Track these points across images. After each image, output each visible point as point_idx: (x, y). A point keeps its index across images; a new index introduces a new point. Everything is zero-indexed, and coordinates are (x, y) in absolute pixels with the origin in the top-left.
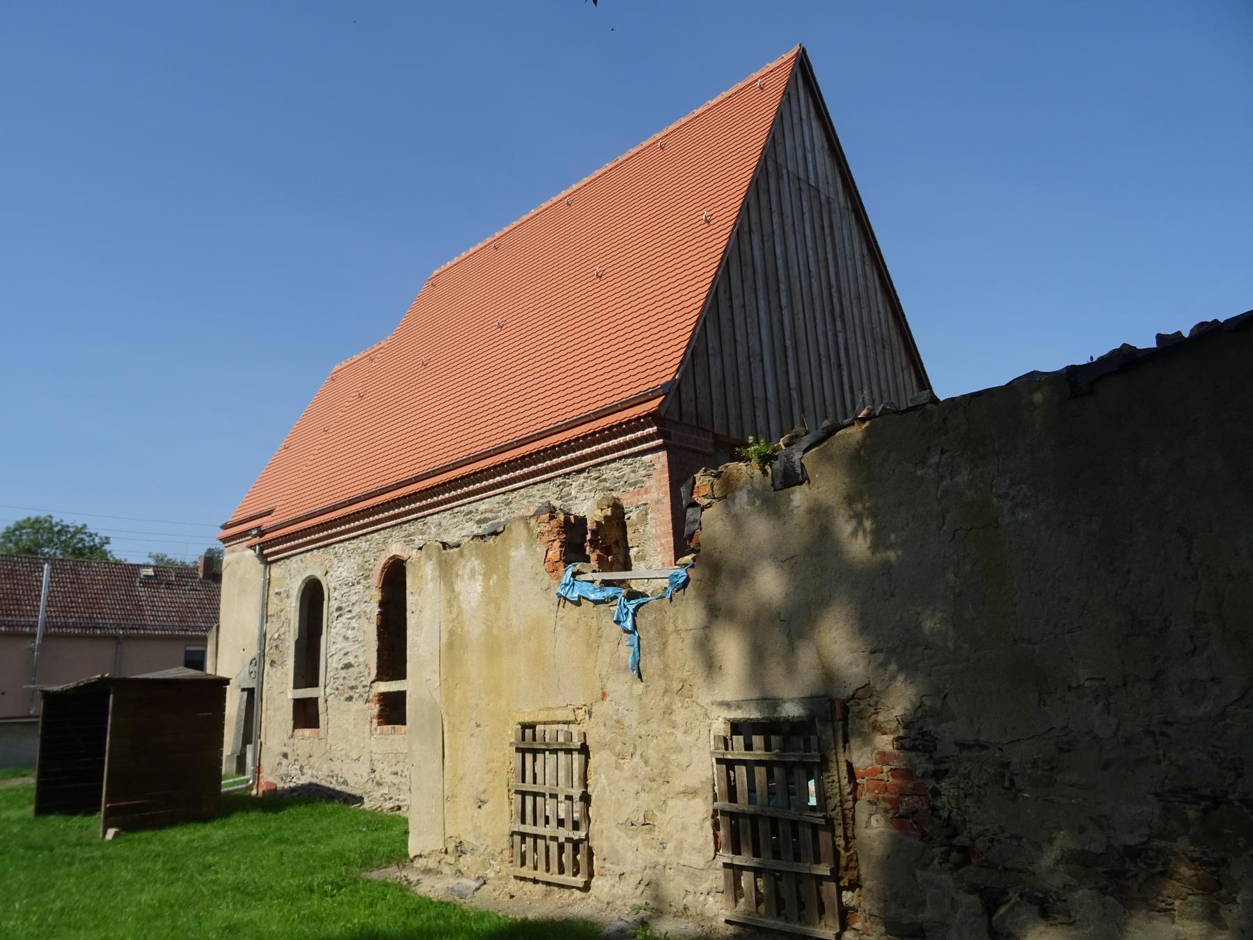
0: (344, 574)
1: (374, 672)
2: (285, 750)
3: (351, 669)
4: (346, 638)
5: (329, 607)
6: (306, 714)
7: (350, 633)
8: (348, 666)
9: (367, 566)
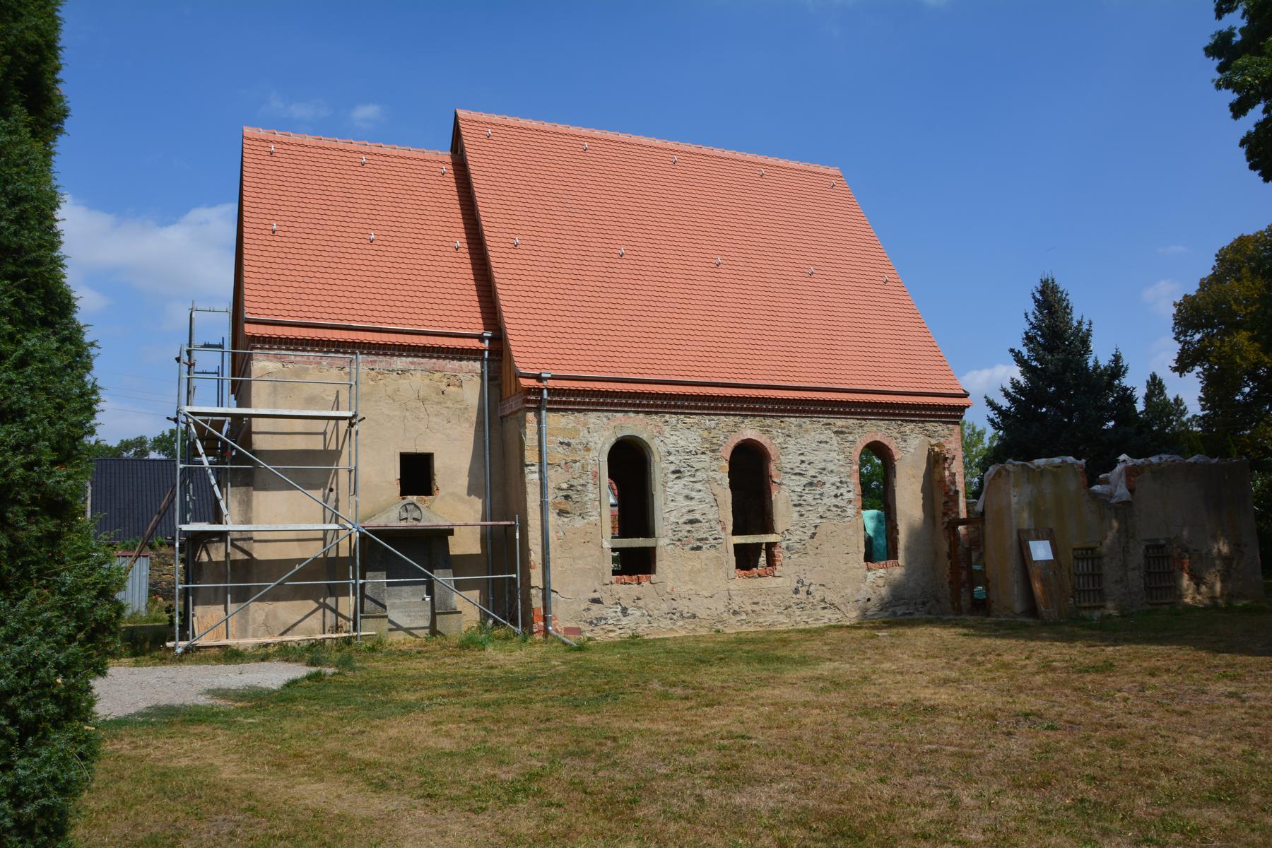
0: (682, 443)
1: (730, 528)
2: (596, 595)
3: (697, 525)
4: (688, 497)
5: (660, 469)
6: (636, 563)
7: (693, 494)
8: (692, 522)
9: (715, 441)
